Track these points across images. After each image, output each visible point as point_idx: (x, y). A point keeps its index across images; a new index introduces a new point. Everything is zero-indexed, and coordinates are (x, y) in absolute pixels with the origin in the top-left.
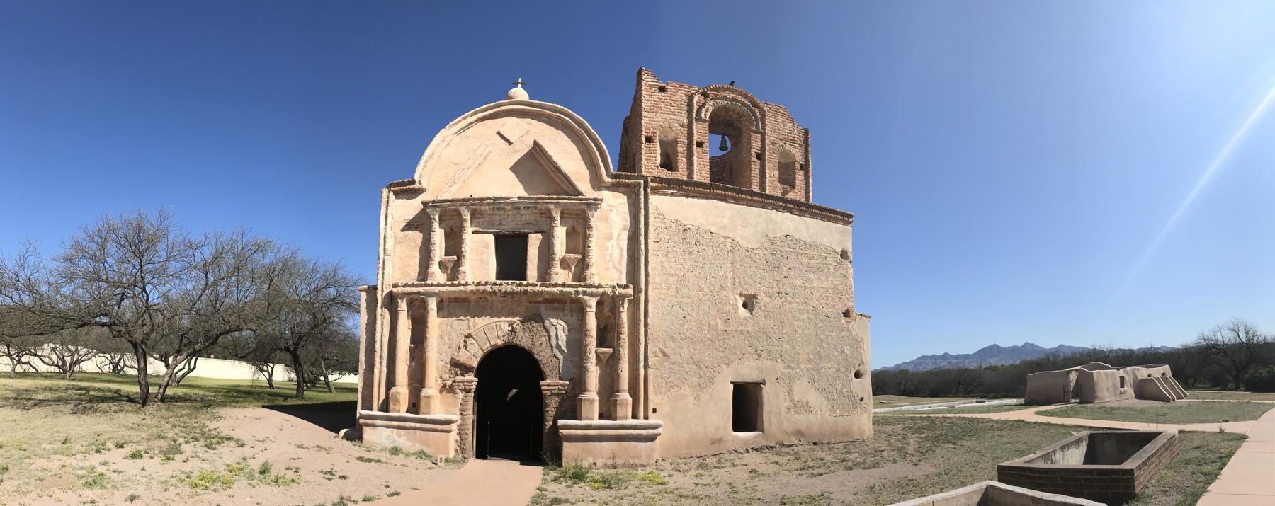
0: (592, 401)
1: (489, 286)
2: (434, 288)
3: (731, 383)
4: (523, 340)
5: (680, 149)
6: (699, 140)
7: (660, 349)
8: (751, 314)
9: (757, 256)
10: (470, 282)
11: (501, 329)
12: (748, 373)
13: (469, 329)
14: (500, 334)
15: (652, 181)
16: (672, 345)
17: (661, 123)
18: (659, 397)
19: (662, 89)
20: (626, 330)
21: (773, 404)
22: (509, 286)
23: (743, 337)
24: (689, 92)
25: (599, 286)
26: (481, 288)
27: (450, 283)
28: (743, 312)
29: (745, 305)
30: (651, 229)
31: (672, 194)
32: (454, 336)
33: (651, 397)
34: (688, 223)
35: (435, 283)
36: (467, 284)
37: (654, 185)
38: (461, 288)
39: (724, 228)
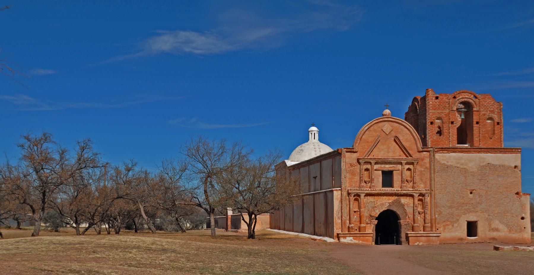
0: (418, 226)
1: (383, 191)
2: (364, 191)
3: (466, 221)
4: (394, 209)
5: (444, 126)
6: (452, 121)
7: (439, 210)
8: (473, 197)
9: (476, 174)
10: (377, 189)
11: (386, 205)
12: (472, 219)
13: (375, 205)
14: (386, 206)
15: (436, 149)
16: (443, 209)
17: (437, 115)
18: (439, 225)
19: (437, 98)
20: (326, 190)
21: (481, 229)
22: (388, 190)
23: (470, 205)
24: (448, 97)
25: (420, 190)
26: (380, 192)
27: (370, 189)
28: (470, 195)
29: (471, 193)
30: (436, 167)
31: (443, 153)
32: (370, 207)
33: (437, 225)
34: (449, 164)
35: (365, 189)
36: (376, 190)
37: (436, 150)
38: (374, 192)
39: (462, 164)
